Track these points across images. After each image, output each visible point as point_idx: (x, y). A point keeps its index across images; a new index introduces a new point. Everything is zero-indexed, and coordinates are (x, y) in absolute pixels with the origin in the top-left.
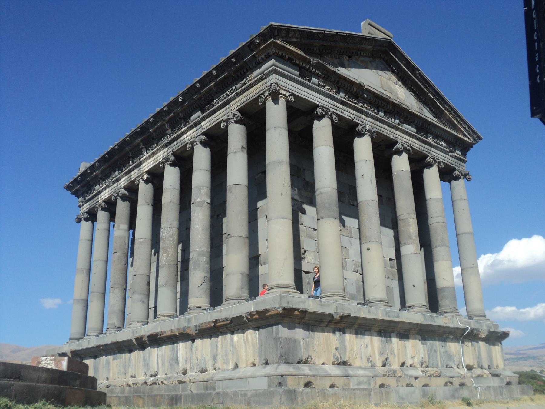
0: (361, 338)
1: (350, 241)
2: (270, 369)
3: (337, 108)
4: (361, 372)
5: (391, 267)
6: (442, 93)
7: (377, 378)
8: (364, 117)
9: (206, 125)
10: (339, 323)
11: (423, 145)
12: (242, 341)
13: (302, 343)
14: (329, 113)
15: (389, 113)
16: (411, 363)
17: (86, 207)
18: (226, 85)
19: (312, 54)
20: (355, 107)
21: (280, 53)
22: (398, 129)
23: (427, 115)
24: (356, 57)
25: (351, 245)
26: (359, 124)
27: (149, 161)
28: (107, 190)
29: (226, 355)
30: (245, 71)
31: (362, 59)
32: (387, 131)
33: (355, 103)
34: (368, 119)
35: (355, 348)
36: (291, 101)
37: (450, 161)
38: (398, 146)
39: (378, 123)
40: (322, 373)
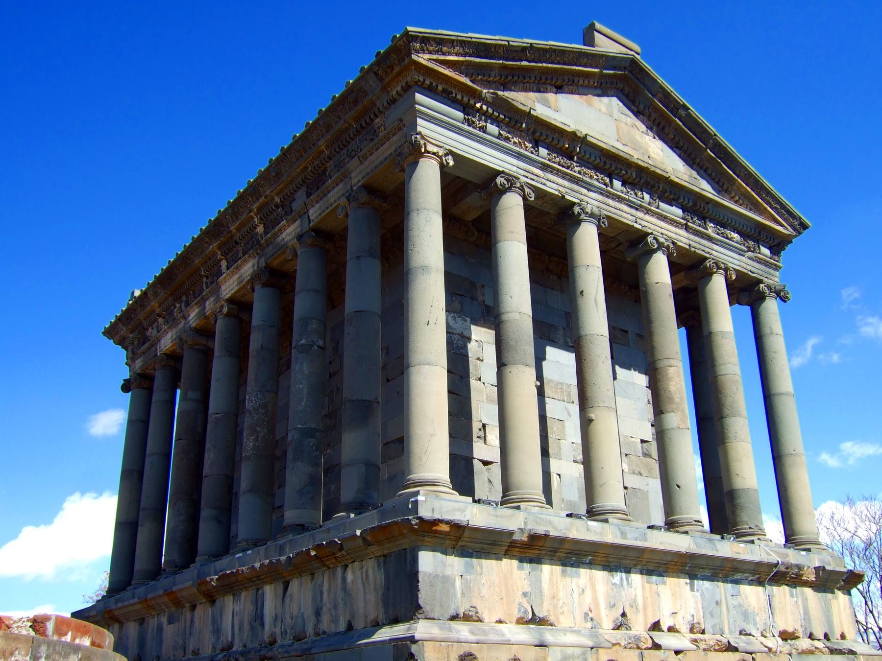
1: (566, 409)
2: (398, 631)
3: (533, 177)
4: (571, 638)
5: (646, 455)
6: (731, 148)
8: (584, 191)
9: (314, 213)
10: (529, 549)
12: (360, 582)
14: (518, 185)
15: (630, 184)
17: (139, 363)
18: (344, 143)
19: (487, 84)
20: (567, 174)
21: (428, 82)
22: (648, 212)
23: (705, 188)
24: (570, 87)
26: (574, 204)
27: (231, 281)
28: (169, 335)
29: (335, 607)
30: (372, 116)
32: (626, 215)
34: (592, 194)
35: (561, 595)
36: (448, 163)
37: (749, 268)
38: (650, 239)
39: (611, 202)
40: (492, 637)
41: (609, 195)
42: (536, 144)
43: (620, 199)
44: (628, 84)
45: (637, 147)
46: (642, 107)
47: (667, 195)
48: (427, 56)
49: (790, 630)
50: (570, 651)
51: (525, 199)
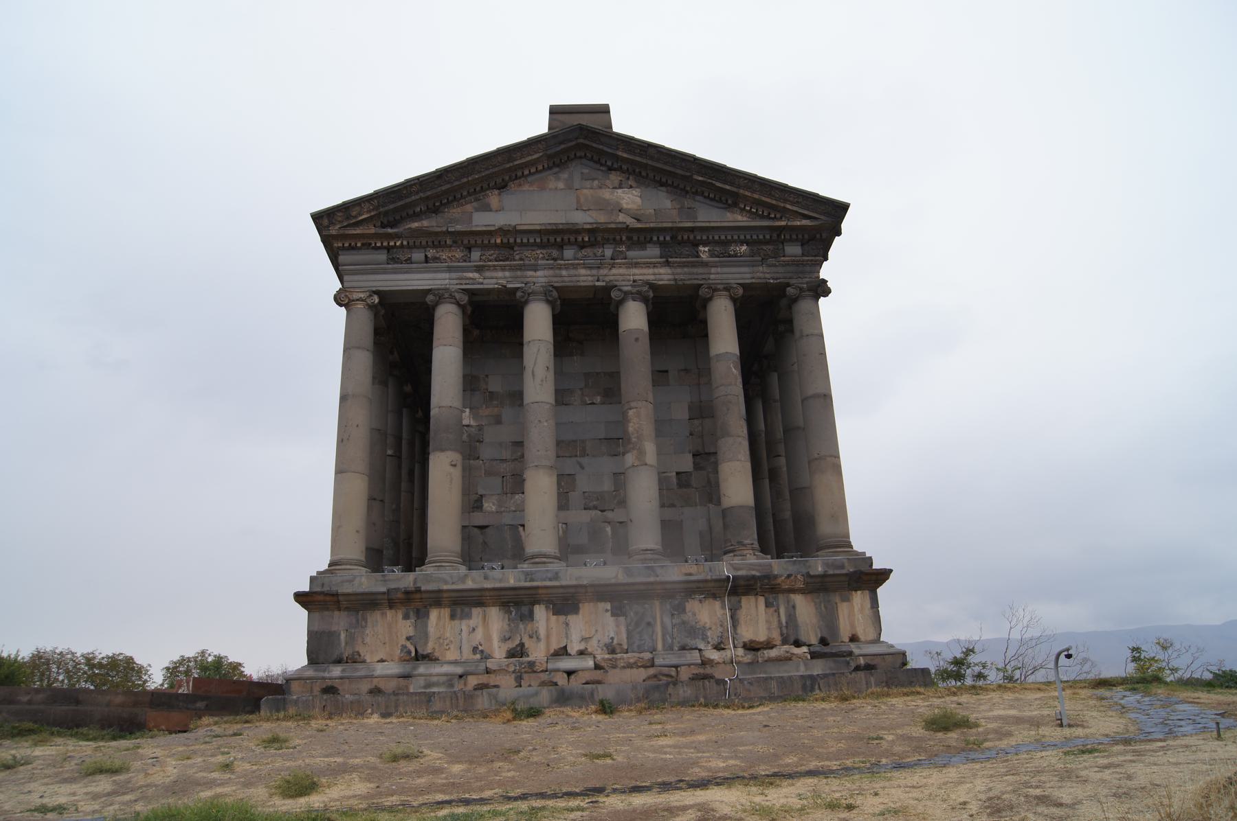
0: (461, 619)
4: (446, 669)
7: (470, 678)
8: (530, 273)
13: (343, 636)
16: (582, 647)
21: (347, 245)
22: (613, 266)
25: (582, 468)
26: (518, 289)
31: (529, 179)
32: (584, 277)
33: (507, 260)
34: (539, 273)
35: (448, 635)
39: (564, 273)
43: (575, 267)
45: (603, 205)
46: (609, 163)
48: (337, 227)
50: (435, 679)
51: (458, 304)
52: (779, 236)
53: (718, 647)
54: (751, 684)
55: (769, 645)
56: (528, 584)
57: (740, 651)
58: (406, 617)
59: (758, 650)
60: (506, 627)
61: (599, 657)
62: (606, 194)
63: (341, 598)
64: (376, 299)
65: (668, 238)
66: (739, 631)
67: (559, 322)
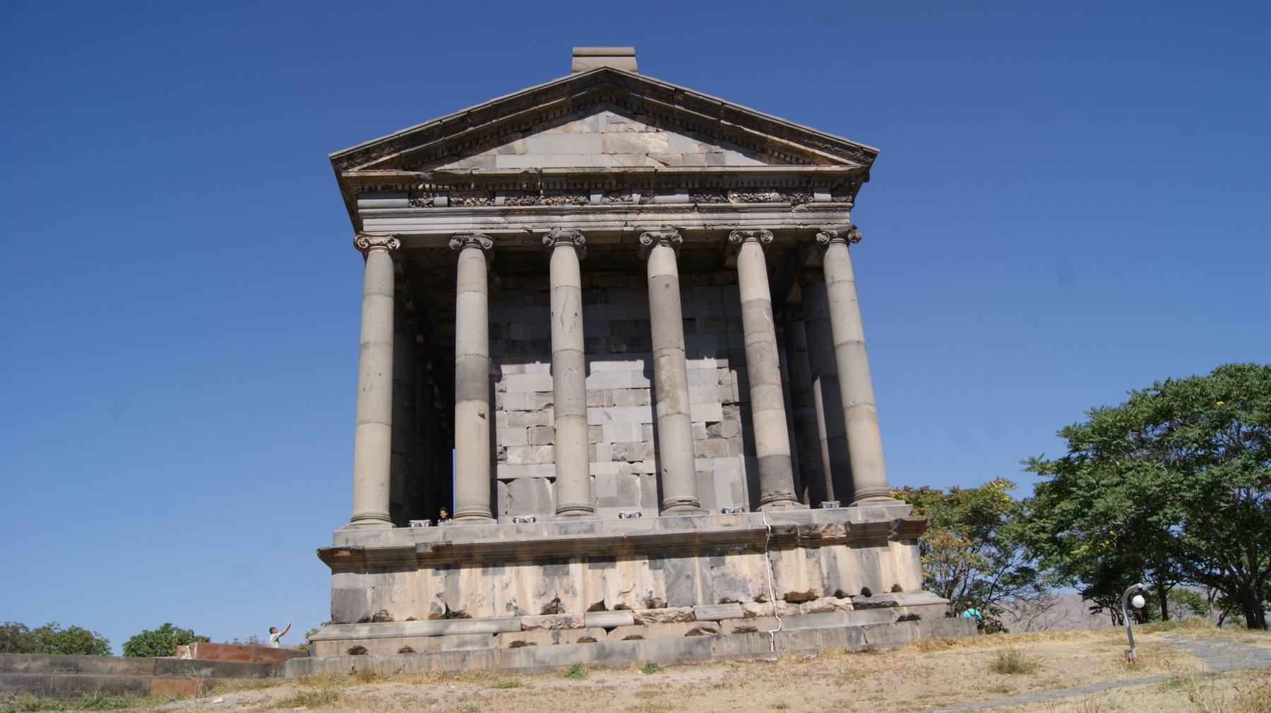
0: (494, 574)
1: (606, 413)
7: (505, 635)
11: (715, 215)
13: (369, 594)
14: (471, 240)
16: (620, 602)
22: (641, 211)
25: (609, 418)
26: (543, 234)
32: (612, 223)
33: (533, 204)
34: (566, 218)
35: (480, 591)
37: (798, 222)
39: (591, 217)
41: (587, 212)
42: (492, 195)
44: (607, 93)
45: (629, 150)
47: (664, 186)
49: (803, 589)
51: (482, 248)
52: (808, 182)
53: (759, 600)
54: (795, 636)
55: (810, 597)
56: (563, 537)
57: (782, 604)
58: (434, 574)
59: (799, 602)
60: (541, 582)
61: (638, 612)
62: (633, 138)
63: (368, 556)
64: (397, 244)
65: (697, 185)
66: (780, 582)
67: (588, 268)
